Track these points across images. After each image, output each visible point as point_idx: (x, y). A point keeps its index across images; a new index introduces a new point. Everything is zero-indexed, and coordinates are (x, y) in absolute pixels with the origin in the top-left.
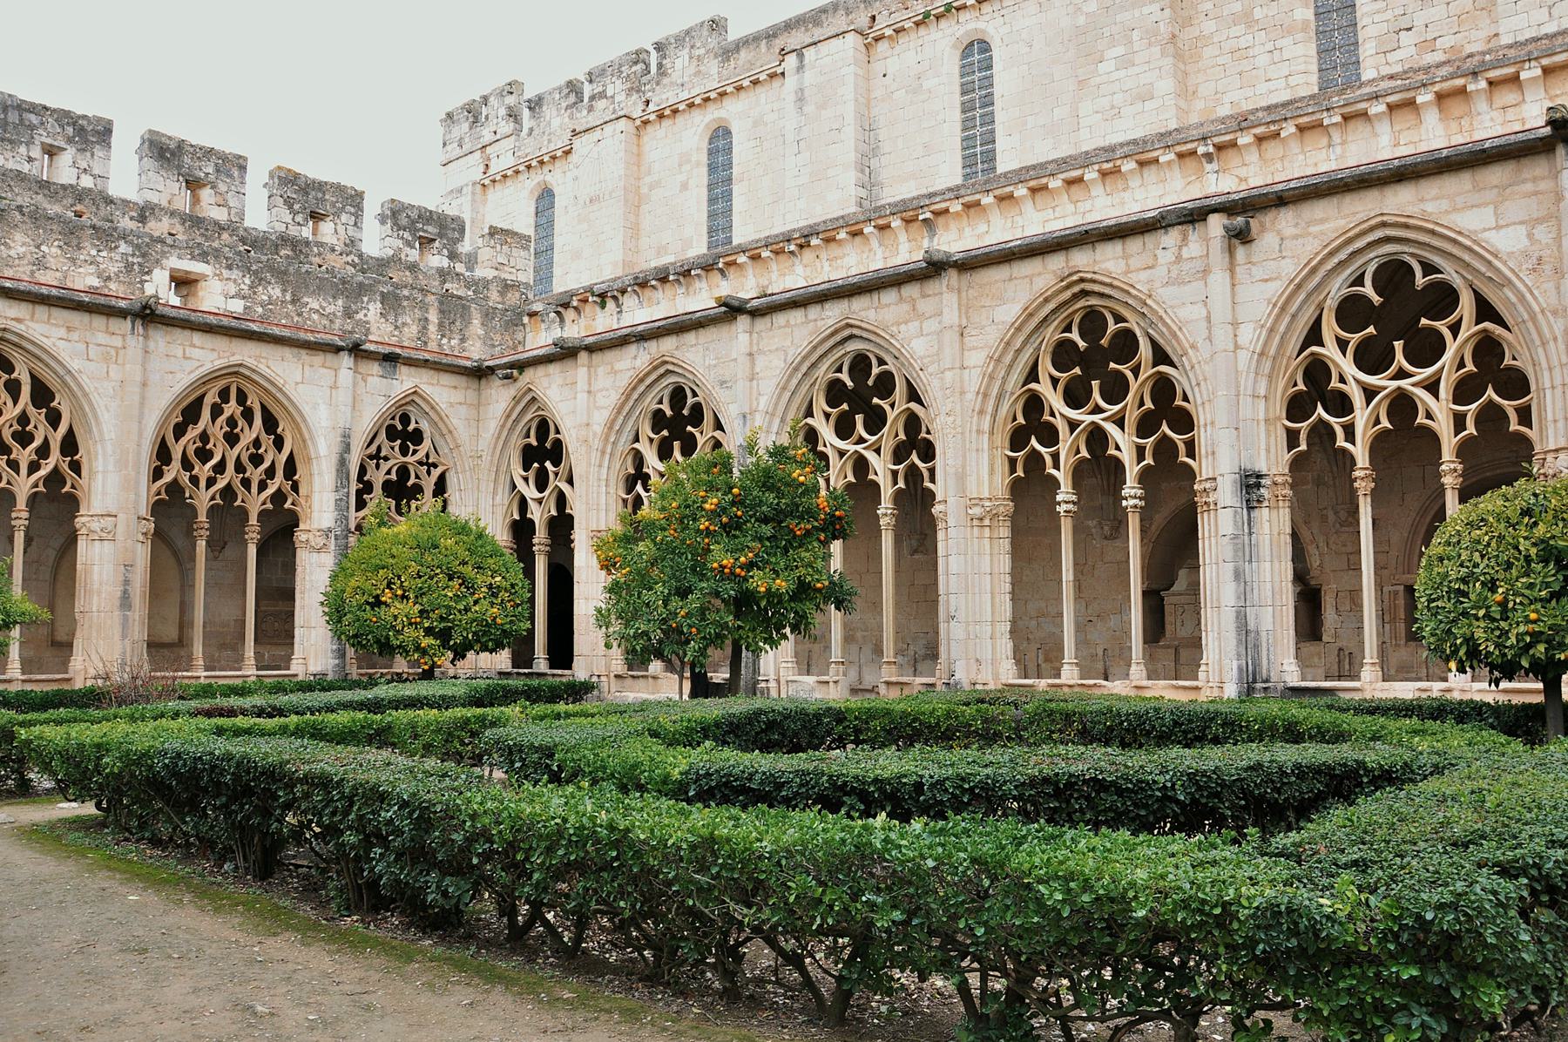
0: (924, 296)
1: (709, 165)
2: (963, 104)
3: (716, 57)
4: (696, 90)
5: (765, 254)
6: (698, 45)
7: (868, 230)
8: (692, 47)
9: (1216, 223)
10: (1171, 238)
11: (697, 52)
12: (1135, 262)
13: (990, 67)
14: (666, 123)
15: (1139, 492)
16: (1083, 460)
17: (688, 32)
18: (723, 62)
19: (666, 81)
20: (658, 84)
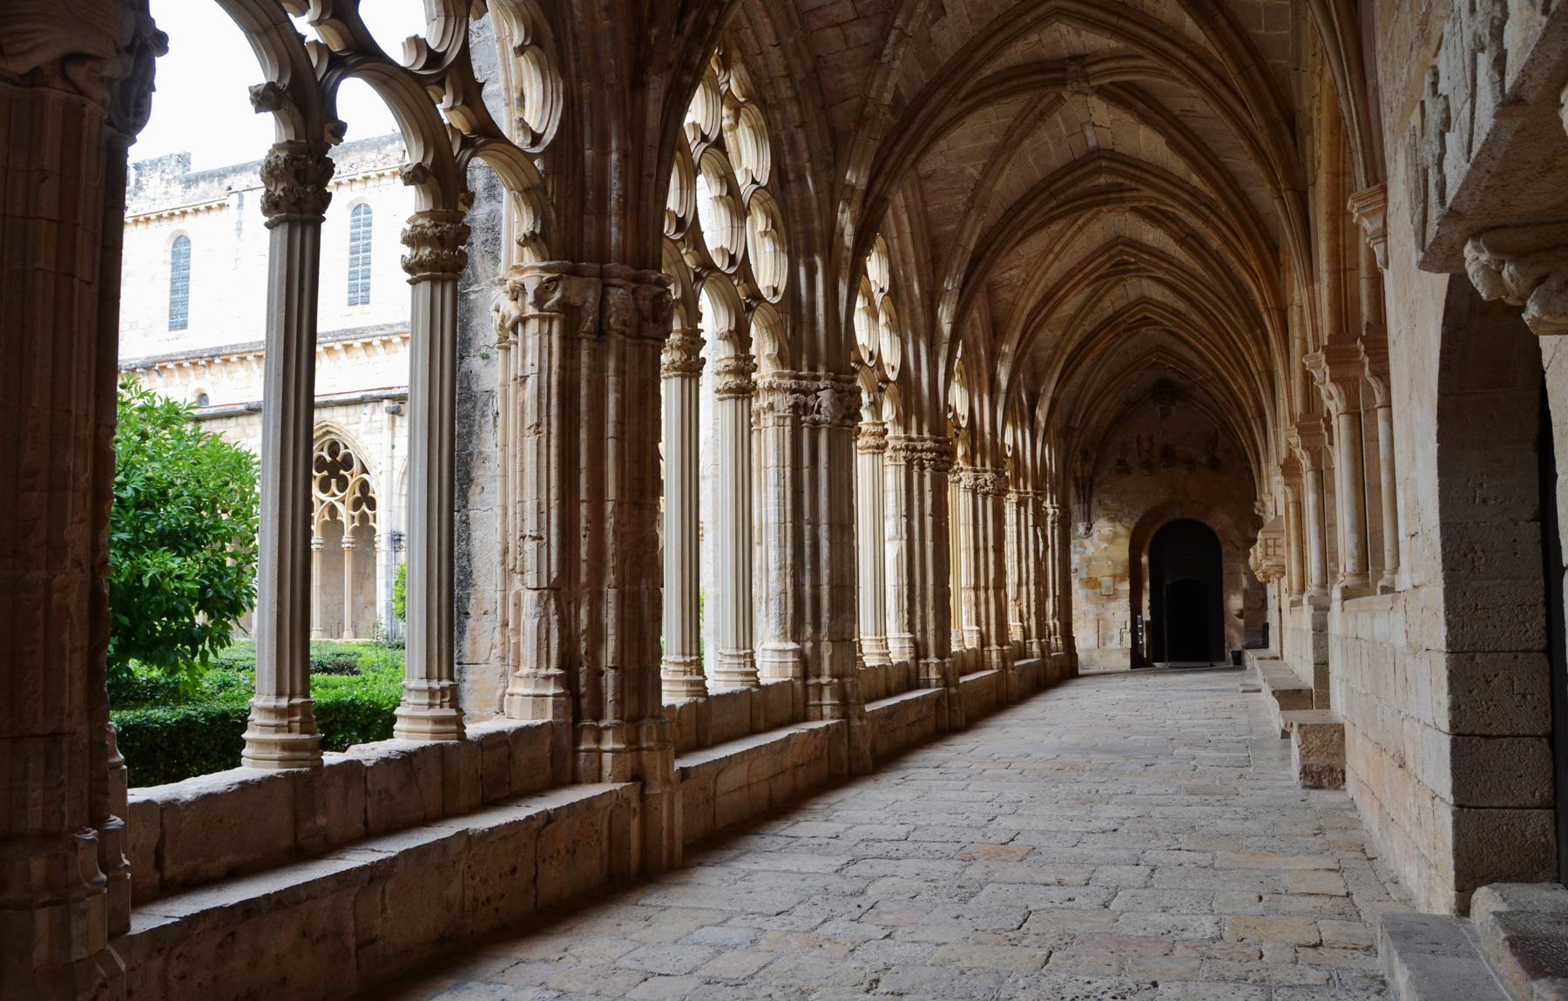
0: (250, 425)
1: (173, 264)
2: (351, 247)
3: (181, 182)
4: (164, 206)
5: (186, 364)
6: (167, 171)
7: (250, 357)
8: (163, 171)
9: (386, 403)
10: (368, 409)
11: (166, 177)
12: (352, 420)
13: (370, 225)
14: (141, 226)
15: (351, 540)
16: (326, 521)
17: (160, 160)
18: (185, 188)
19: (141, 194)
20: (135, 195)
